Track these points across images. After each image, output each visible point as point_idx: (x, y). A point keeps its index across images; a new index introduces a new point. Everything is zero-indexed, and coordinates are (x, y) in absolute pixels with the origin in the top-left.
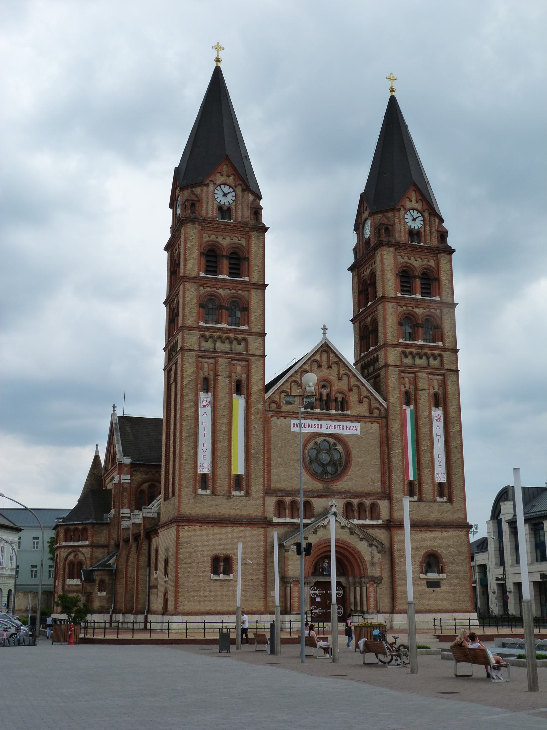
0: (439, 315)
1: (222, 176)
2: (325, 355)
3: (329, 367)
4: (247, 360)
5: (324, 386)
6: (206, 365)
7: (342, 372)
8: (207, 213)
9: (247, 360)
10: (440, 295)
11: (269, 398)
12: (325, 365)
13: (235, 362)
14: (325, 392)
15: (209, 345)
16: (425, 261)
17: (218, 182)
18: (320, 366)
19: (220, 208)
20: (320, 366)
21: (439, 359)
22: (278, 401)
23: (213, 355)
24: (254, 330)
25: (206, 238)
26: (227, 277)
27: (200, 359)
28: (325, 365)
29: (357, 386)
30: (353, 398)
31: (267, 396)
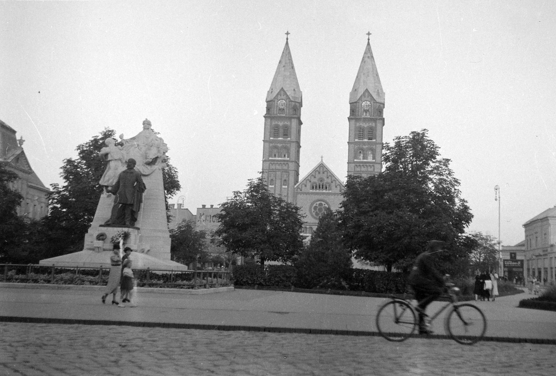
0: (375, 148)
1: (281, 96)
2: (322, 168)
3: (323, 173)
4: (288, 172)
5: (321, 181)
6: (272, 175)
7: (328, 175)
8: (274, 113)
9: (288, 172)
10: (375, 138)
11: (297, 187)
12: (321, 173)
13: (283, 173)
14: (321, 183)
15: (273, 167)
16: (370, 124)
17: (279, 99)
18: (319, 173)
19: (280, 109)
20: (319, 173)
21: (373, 167)
22: (301, 188)
23: (275, 171)
24: (291, 160)
25: (273, 123)
26: (282, 139)
27: (270, 172)
28: (321, 173)
29: (335, 180)
30: (333, 185)
31: (296, 186)
